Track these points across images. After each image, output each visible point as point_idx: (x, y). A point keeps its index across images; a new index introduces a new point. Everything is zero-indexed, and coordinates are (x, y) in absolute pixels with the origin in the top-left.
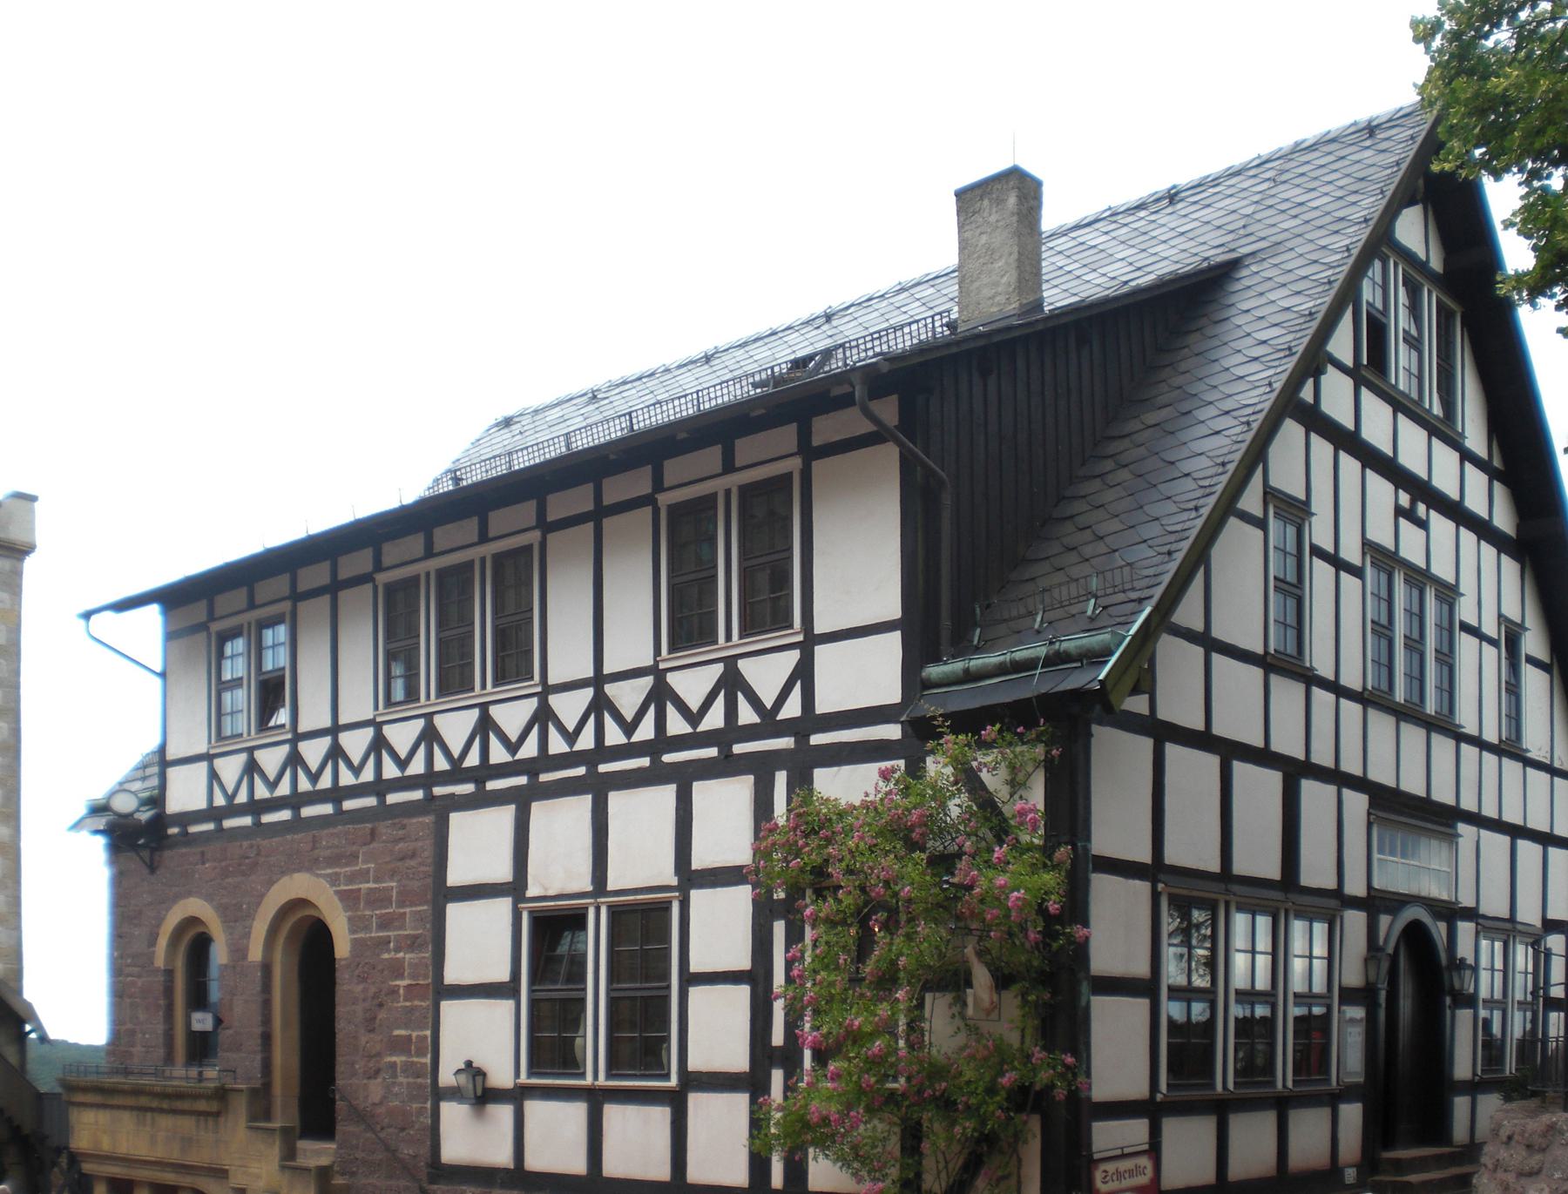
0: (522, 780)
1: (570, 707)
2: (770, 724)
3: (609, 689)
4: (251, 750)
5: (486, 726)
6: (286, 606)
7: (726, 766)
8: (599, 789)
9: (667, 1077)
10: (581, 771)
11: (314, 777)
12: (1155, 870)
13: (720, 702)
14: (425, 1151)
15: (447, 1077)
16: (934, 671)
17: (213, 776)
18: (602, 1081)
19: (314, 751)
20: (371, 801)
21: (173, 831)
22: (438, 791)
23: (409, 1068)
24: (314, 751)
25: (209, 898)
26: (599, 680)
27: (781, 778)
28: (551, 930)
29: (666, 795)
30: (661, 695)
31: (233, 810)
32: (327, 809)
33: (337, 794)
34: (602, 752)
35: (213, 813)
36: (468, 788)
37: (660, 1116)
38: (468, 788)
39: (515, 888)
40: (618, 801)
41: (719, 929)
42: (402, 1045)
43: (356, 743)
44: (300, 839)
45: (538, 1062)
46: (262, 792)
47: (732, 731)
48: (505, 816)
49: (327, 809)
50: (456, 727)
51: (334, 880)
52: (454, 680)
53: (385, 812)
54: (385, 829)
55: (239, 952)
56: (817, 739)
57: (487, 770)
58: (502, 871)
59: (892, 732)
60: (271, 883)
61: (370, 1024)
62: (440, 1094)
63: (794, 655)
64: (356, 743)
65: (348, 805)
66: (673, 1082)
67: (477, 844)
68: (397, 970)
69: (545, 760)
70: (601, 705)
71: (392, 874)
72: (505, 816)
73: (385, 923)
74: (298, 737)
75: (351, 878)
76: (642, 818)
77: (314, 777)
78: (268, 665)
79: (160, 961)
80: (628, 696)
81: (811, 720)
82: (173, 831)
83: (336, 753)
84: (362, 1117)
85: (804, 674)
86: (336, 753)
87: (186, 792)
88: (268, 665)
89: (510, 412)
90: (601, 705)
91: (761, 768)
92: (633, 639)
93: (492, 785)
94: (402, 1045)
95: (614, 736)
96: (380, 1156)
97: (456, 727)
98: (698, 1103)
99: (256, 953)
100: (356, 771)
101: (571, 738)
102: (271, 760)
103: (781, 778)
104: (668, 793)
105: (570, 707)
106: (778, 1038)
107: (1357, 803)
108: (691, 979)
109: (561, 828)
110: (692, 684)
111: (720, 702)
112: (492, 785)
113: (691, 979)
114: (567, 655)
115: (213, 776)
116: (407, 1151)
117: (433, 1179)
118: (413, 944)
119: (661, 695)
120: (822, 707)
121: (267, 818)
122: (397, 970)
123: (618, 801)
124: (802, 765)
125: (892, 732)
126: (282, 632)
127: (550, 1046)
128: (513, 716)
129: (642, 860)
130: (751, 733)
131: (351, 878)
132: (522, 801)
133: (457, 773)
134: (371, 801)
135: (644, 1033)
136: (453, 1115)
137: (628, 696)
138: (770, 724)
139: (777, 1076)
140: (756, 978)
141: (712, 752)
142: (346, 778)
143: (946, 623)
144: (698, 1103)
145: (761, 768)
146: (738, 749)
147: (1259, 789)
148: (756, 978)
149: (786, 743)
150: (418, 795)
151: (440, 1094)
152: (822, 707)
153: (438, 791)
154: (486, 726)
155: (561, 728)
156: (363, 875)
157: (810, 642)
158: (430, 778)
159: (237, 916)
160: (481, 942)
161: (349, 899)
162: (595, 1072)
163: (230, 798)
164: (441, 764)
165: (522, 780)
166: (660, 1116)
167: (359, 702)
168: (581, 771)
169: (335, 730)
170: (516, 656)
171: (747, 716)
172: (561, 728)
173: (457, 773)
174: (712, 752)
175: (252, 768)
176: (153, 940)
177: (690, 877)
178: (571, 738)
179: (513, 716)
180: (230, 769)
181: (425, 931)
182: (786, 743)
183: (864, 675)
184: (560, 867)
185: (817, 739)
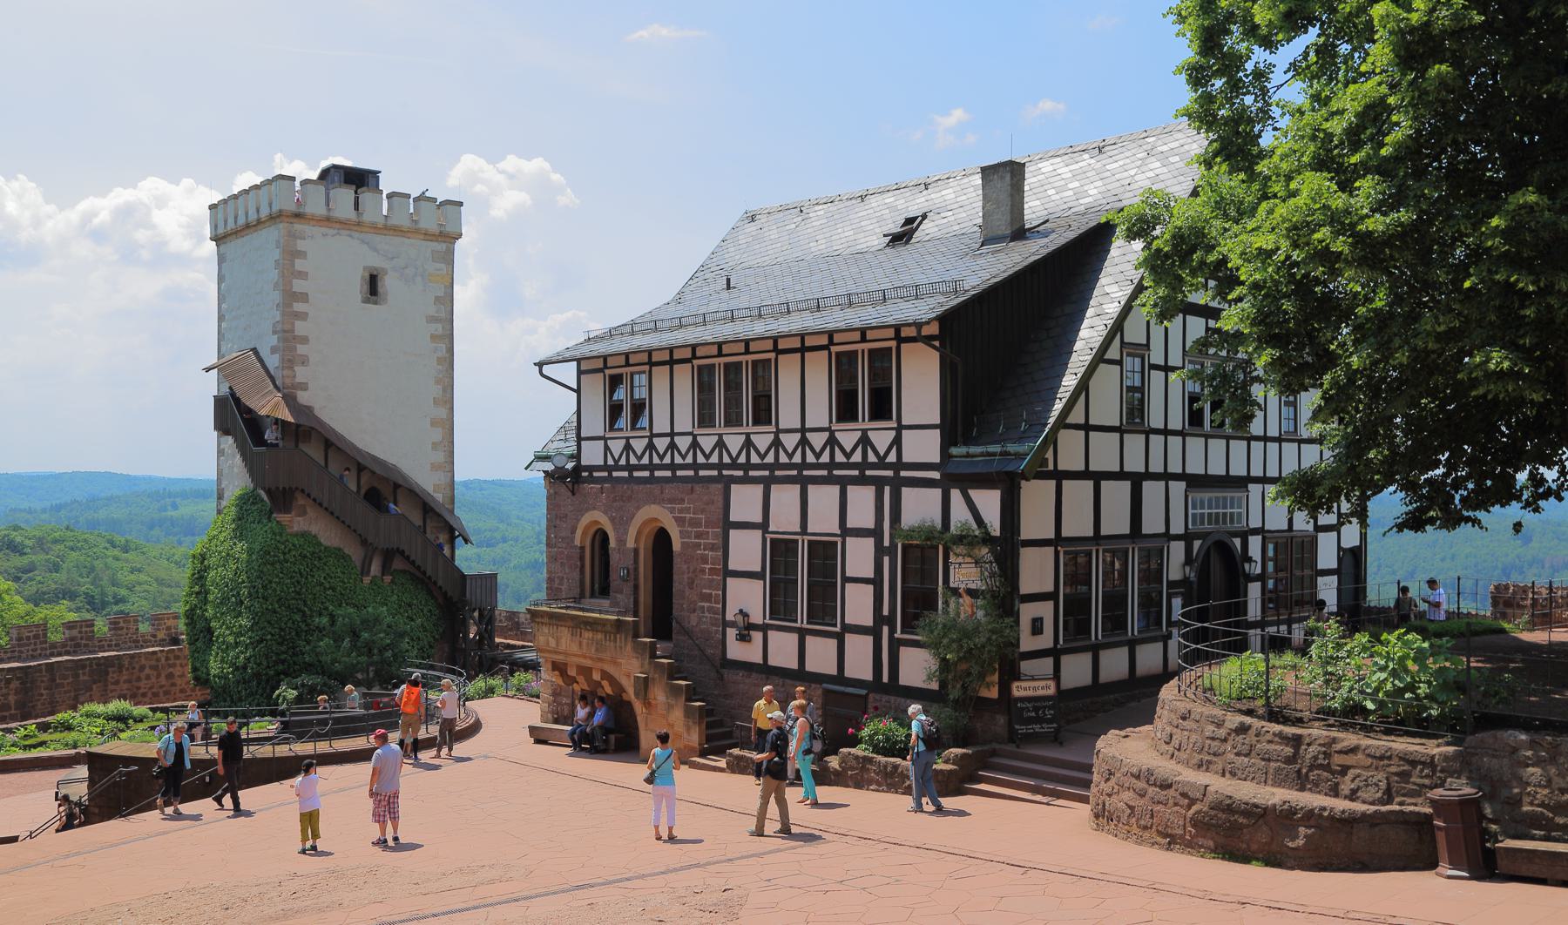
0: (767, 473)
1: (790, 441)
2: (882, 464)
3: (808, 435)
4: (628, 439)
5: (748, 444)
6: (647, 368)
7: (862, 481)
8: (804, 483)
9: (835, 625)
10: (795, 472)
11: (661, 457)
12: (1058, 541)
13: (860, 449)
14: (719, 652)
15: (729, 617)
16: (954, 451)
17: (607, 448)
18: (805, 626)
19: (661, 443)
20: (691, 473)
21: (585, 474)
22: (725, 472)
23: (710, 610)
24: (661, 443)
25: (605, 513)
26: (803, 430)
27: (887, 489)
28: (780, 551)
29: (836, 489)
30: (832, 442)
31: (617, 467)
32: (668, 474)
33: (673, 467)
34: (804, 465)
35: (605, 467)
36: (740, 473)
37: (833, 643)
38: (740, 473)
39: (764, 526)
40: (812, 490)
41: (859, 557)
42: (708, 598)
43: (683, 443)
44: (656, 488)
45: (774, 613)
46: (633, 461)
47: (864, 465)
48: (759, 489)
49: (668, 474)
50: (734, 442)
51: (672, 511)
52: (733, 420)
53: (697, 479)
54: (698, 488)
55: (621, 542)
56: (903, 474)
57: (748, 466)
58: (758, 518)
59: (936, 475)
60: (638, 508)
61: (691, 583)
62: (726, 624)
63: (893, 433)
64: (683, 443)
65: (679, 473)
66: (838, 629)
67: (745, 502)
68: (704, 560)
69: (777, 465)
70: (804, 442)
71: (703, 511)
72: (759, 489)
73: (699, 535)
74: (652, 436)
75: (681, 511)
76: (824, 499)
77: (661, 457)
78: (637, 396)
79: (577, 542)
80: (818, 440)
81: (900, 465)
82: (585, 474)
83: (672, 446)
84: (687, 633)
85: (897, 442)
86: (672, 446)
87: (592, 455)
88: (637, 396)
89: (753, 207)
90: (804, 442)
91: (879, 483)
92: (820, 411)
93: (752, 473)
94: (708, 598)
95: (810, 458)
96: (697, 652)
97: (734, 442)
98: (850, 639)
99: (630, 544)
100: (684, 457)
101: (790, 456)
102: (639, 445)
103: (887, 489)
104: (836, 489)
105: (790, 441)
106: (886, 612)
107: (1178, 487)
108: (846, 580)
109: (785, 499)
110: (848, 439)
111: (860, 449)
112: (752, 473)
113: (846, 580)
114: (788, 415)
115: (607, 448)
116: (710, 651)
117: (723, 666)
118: (713, 548)
119: (832, 442)
120: (905, 459)
121: (636, 474)
122: (704, 560)
123: (812, 490)
124: (898, 484)
125: (936, 475)
126: (644, 377)
127: (780, 605)
128: (762, 441)
129: (824, 519)
130: (873, 466)
131: (681, 511)
132: (767, 483)
133: (734, 465)
134: (691, 473)
135: (825, 605)
136: (731, 633)
137: (818, 440)
138: (882, 464)
139: (886, 629)
140: (876, 582)
141: (856, 473)
142: (678, 460)
143: (960, 428)
144: (850, 639)
145: (879, 483)
146: (868, 473)
147: (1117, 495)
148: (876, 582)
149: (890, 473)
150: (715, 473)
151: (726, 624)
152: (905, 459)
153: (725, 472)
154: (748, 444)
155: (785, 451)
156: (688, 510)
157: (900, 428)
158: (720, 466)
159: (621, 523)
160: (746, 550)
161: (680, 521)
162: (802, 621)
163: (616, 462)
164: (726, 460)
165: (767, 473)
166: (833, 643)
167: (684, 421)
168: (795, 472)
169: (672, 434)
170: (764, 412)
171: (872, 458)
172: (785, 451)
173: (734, 465)
174: (856, 473)
175: (628, 447)
176: (573, 532)
177: (846, 532)
178: (790, 456)
179: (762, 441)
180: (617, 447)
181: (719, 542)
182: (890, 473)
183: (924, 447)
184: (785, 518)
185: (903, 474)
